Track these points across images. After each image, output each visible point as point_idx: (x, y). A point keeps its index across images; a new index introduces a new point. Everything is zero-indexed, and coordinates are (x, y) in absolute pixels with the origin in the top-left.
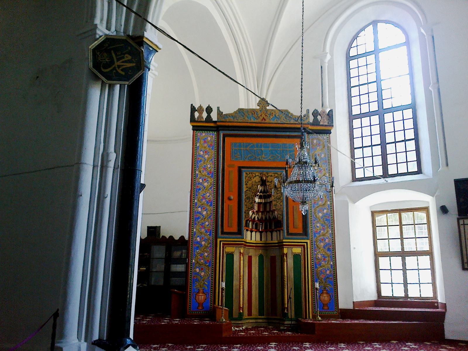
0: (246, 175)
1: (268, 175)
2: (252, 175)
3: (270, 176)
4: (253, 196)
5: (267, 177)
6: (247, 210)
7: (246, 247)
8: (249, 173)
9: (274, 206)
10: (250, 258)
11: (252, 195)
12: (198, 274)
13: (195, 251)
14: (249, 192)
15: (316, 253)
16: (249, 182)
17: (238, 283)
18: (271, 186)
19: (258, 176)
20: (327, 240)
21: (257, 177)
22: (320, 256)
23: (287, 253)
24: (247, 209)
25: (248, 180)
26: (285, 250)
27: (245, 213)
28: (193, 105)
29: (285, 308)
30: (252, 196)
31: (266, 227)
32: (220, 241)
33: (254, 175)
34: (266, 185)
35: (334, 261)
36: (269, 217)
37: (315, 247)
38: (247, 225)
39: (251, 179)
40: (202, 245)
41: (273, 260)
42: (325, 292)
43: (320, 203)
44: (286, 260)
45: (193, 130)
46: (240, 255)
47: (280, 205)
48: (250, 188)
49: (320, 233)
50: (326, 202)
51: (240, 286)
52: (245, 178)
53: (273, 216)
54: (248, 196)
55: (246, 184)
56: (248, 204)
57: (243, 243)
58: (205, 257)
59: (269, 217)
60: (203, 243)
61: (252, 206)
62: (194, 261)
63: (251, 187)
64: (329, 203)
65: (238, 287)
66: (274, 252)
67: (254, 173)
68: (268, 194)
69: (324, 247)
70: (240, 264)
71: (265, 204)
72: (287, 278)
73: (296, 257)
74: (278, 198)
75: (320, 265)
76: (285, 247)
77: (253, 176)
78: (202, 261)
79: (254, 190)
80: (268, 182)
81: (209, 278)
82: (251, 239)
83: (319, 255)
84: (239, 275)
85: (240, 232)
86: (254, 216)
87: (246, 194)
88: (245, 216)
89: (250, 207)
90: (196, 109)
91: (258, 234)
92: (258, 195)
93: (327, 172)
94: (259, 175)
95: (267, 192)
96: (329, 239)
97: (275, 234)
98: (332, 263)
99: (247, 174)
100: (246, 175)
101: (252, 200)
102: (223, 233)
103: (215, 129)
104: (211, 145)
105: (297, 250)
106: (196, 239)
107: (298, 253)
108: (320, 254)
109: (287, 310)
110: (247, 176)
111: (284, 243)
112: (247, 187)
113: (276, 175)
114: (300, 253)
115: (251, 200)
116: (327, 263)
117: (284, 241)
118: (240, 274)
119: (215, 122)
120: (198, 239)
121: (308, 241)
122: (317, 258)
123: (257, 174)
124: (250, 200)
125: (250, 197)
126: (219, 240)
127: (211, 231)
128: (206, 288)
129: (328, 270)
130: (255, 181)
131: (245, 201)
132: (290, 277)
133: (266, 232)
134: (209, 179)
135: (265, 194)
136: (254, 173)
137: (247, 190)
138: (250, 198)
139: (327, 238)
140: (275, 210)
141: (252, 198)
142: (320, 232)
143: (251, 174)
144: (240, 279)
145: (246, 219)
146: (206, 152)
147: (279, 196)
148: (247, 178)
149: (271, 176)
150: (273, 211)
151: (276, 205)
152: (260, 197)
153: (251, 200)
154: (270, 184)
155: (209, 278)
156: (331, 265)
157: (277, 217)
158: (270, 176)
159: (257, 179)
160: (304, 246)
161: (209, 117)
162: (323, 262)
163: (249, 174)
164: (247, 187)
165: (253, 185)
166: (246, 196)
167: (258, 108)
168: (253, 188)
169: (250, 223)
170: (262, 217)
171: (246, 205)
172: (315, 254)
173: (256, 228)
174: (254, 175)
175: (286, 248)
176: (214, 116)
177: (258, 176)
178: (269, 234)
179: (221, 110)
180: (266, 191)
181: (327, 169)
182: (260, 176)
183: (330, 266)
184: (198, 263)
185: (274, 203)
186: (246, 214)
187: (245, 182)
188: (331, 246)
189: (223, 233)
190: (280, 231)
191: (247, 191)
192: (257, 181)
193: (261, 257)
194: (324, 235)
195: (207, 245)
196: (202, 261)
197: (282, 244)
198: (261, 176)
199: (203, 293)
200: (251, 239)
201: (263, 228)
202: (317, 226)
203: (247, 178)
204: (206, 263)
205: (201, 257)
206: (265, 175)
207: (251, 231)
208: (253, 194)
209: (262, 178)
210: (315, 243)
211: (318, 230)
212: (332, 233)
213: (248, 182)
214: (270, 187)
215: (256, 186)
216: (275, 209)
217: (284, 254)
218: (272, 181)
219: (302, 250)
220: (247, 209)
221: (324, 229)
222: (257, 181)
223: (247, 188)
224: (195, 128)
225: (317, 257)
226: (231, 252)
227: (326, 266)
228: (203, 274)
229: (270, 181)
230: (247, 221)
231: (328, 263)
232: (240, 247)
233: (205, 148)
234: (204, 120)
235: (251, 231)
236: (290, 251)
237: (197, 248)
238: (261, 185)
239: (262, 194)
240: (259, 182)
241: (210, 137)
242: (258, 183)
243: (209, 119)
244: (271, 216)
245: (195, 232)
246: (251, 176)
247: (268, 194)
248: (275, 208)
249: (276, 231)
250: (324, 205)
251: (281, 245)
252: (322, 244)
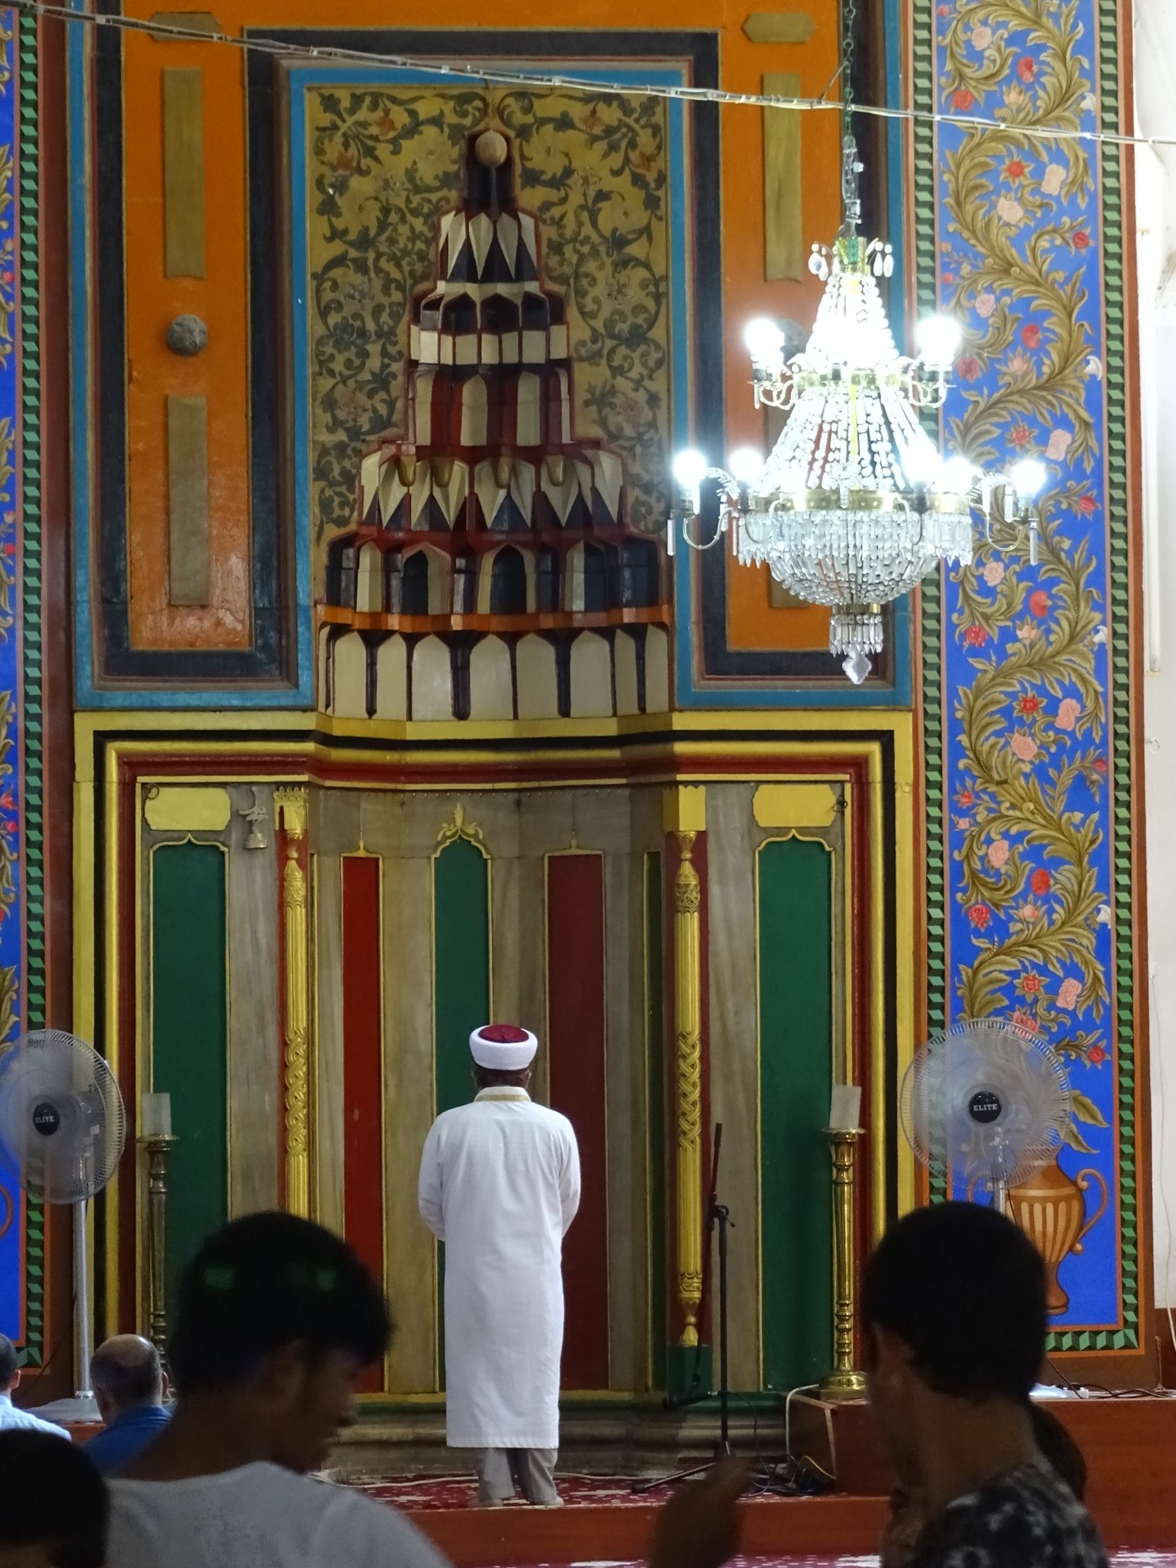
0: (326, 119)
1: (528, 110)
2: (379, 113)
3: (549, 127)
4: (396, 317)
5: (524, 132)
6: (341, 448)
7: (328, 783)
8: (357, 100)
9: (587, 403)
10: (361, 881)
11: (378, 310)
14: (358, 279)
15: (963, 824)
16: (356, 182)
17: (269, 1101)
18: (558, 223)
19: (437, 121)
20: (1068, 714)
21: (430, 131)
22: (999, 855)
23: (702, 836)
24: (341, 436)
25: (343, 163)
26: (691, 809)
29: (679, 1311)
30: (385, 317)
31: (510, 597)
33: (400, 117)
34: (509, 206)
35: (1124, 897)
36: (540, 498)
37: (956, 771)
38: (337, 589)
39: (370, 152)
41: (572, 891)
42: (1038, 1163)
43: (1017, 365)
44: (694, 895)
46: (283, 859)
47: (642, 396)
48: (364, 242)
49: (1010, 648)
50: (1066, 360)
51: (284, 1131)
52: (319, 151)
53: (580, 498)
54: (347, 311)
55: (328, 207)
57: (309, 747)
59: (540, 498)
61: (383, 410)
63: (373, 232)
64: (1095, 366)
65: (272, 1138)
66: (596, 825)
67: (397, 93)
68: (532, 287)
69: (1040, 771)
71: (502, 380)
72: (705, 1058)
73: (790, 862)
74: (623, 328)
75: (1000, 929)
76: (686, 783)
77: (386, 122)
79: (406, 253)
80: (532, 178)
82: (371, 711)
83: (989, 841)
84: (272, 1031)
86: (397, 492)
87: (328, 296)
88: (325, 506)
91: (433, 661)
92: (434, 305)
93: (1086, 74)
94: (451, 118)
95: (524, 269)
96: (1090, 703)
97: (589, 655)
98: (1106, 915)
99: (330, 104)
100: (326, 119)
101: (384, 353)
105: (800, 806)
107: (802, 830)
108: (1006, 835)
109: (703, 1328)
110: (335, 127)
111: (682, 748)
112: (335, 234)
113: (610, 115)
114: (824, 831)
115: (374, 348)
116: (1060, 914)
117: (682, 721)
121: (901, 725)
122: (973, 873)
123: (425, 110)
124: (364, 355)
125: (371, 326)
129: (1072, 971)
130: (411, 174)
131: (324, 365)
132: (726, 1043)
133: (511, 639)
135: (502, 289)
136: (394, 100)
137: (338, 261)
138: (362, 333)
139: (1071, 692)
140: (596, 444)
141: (386, 336)
142: (1008, 635)
143: (374, 106)
144: (284, 1066)
145: (333, 532)
147: (639, 309)
148: (334, 149)
149: (564, 123)
150: (580, 452)
151: (602, 399)
152: (457, 317)
153: (374, 348)
154: (547, 206)
156: (1102, 933)
157: (613, 510)
158: (549, 127)
159: (431, 156)
160: (859, 766)
162: (1027, 911)
163: (352, 111)
164: (335, 234)
165: (394, 217)
166: (324, 313)
168: (392, 241)
169: (366, 561)
170: (471, 506)
171: (330, 403)
172: (958, 839)
173: (415, 603)
174: (400, 117)
175: (702, 788)
177: (437, 121)
178: (538, 655)
180: (510, 258)
181: (1084, 47)
182: (453, 127)
183: (1088, 940)
185: (584, 375)
186: (332, 484)
187: (320, 184)
188: (1101, 760)
190: (638, 632)
191: (336, 273)
192: (427, 174)
193: (461, 870)
194: (1040, 664)
197: (657, 750)
198: (468, 121)
200: (371, 711)
201: (484, 604)
202: (980, 578)
203: (334, 149)
206: (500, 112)
207: (374, 638)
208: (397, 296)
209: (472, 140)
210: (963, 739)
211: (987, 618)
212: (1121, 645)
213: (342, 186)
214: (549, 232)
215: (419, 224)
216: (596, 432)
217: (673, 839)
218: (568, 172)
219: (841, 803)
220: (341, 436)
221: (1044, 617)
222: (427, 174)
223: (330, 240)
225: (977, 865)
226: (198, 833)
227: (1053, 944)
229: (554, 167)
230: (337, 548)
231: (1071, 913)
232: (278, 785)
235: (374, 638)
236: (737, 820)
238: (469, 208)
239: (473, 291)
240: (446, 180)
242: (434, 197)
244: (555, 496)
246: (374, 130)
247: (529, 298)
248: (603, 423)
249: (607, 633)
250: (1050, 385)
251: (645, 761)
252: (1025, 748)
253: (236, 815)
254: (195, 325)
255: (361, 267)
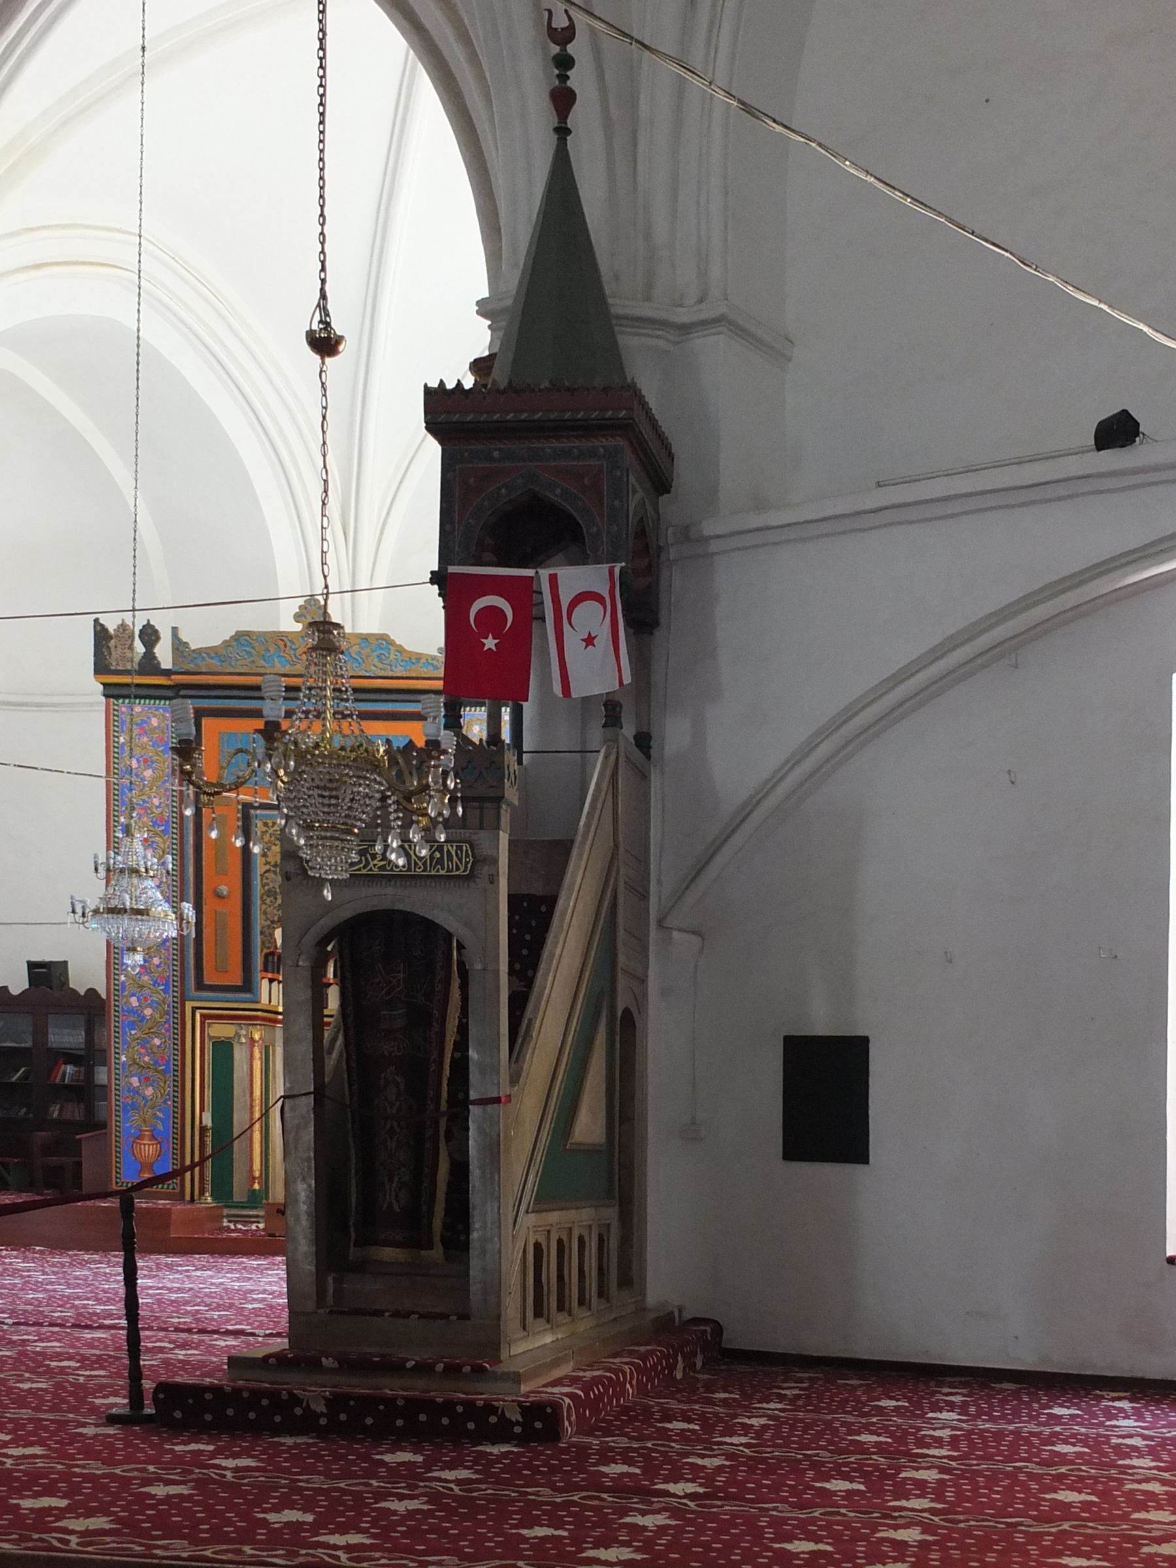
0: (265, 829)
6: (269, 926)
12: (136, 1091)
13: (125, 1033)
16: (273, 847)
25: (270, 842)
27: (262, 933)
28: (101, 621)
32: (194, 1009)
40: (144, 1018)
45: (106, 696)
56: (269, 910)
58: (155, 1050)
60: (148, 1012)
62: (124, 1058)
70: (248, 1067)
78: (147, 1059)
81: (165, 1102)
84: (248, 1096)
85: (248, 986)
88: (263, 943)
89: (276, 919)
90: (111, 631)
99: (266, 824)
102: (200, 986)
103: (169, 693)
104: (162, 740)
106: (128, 1002)
118: (252, 1093)
119: (167, 673)
120: (134, 1001)
126: (189, 1006)
127: (167, 981)
128: (160, 1127)
131: (263, 902)
134: (158, 839)
144: (252, 1106)
145: (265, 951)
146: (145, 761)
155: (165, 1102)
161: (149, 656)
164: (267, 863)
166: (263, 886)
167: (298, 627)
171: (265, 913)
176: (164, 655)
179: (184, 637)
184: (135, 1063)
189: (200, 986)
195: (157, 1016)
196: (147, 1059)
199: (153, 1137)
204: (156, 1063)
205: (143, 1047)
213: (269, 849)
224: (112, 692)
228: (149, 1092)
233: (143, 748)
234: (136, 667)
237: (132, 1025)
241: (157, 718)
243: (149, 664)
245: (123, 983)
253: (237, 1033)
254: (224, 890)
255: (275, 873)
